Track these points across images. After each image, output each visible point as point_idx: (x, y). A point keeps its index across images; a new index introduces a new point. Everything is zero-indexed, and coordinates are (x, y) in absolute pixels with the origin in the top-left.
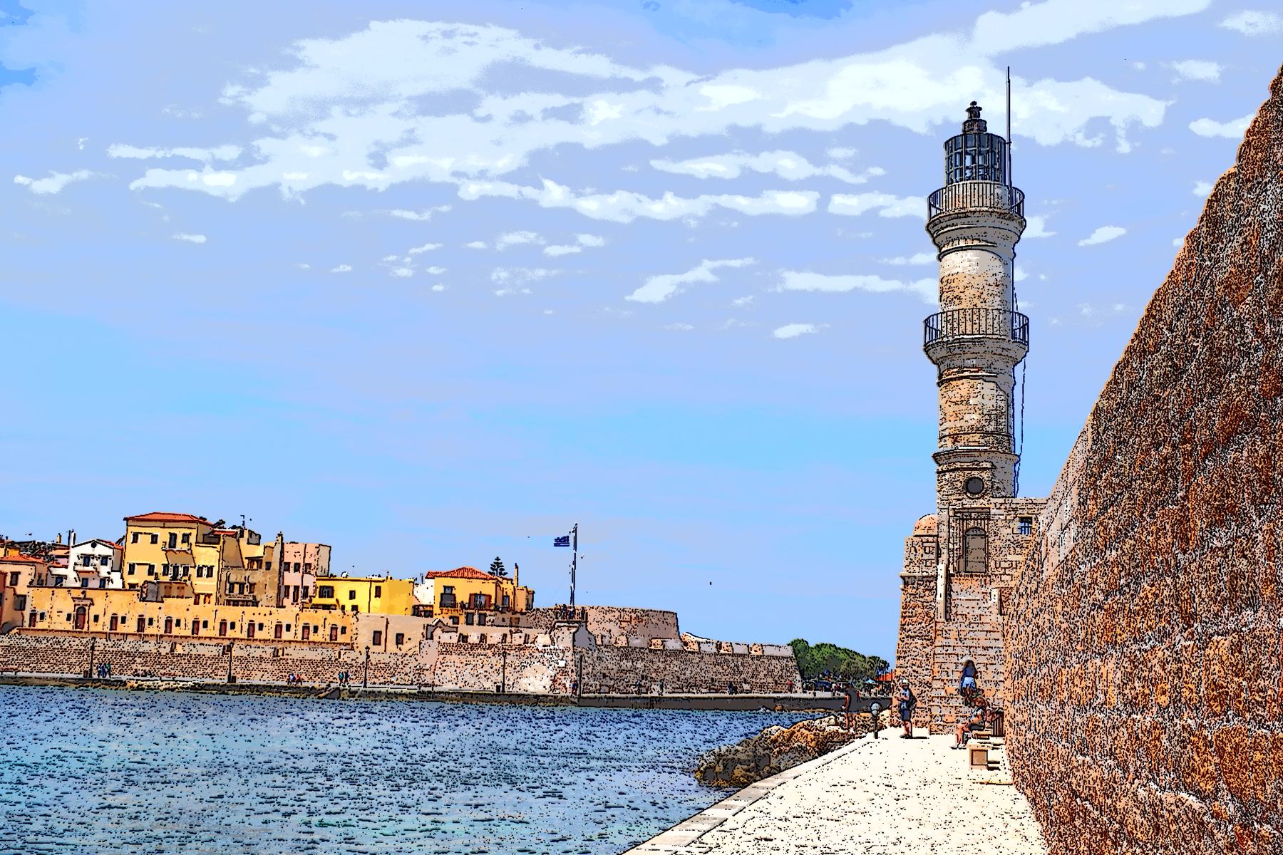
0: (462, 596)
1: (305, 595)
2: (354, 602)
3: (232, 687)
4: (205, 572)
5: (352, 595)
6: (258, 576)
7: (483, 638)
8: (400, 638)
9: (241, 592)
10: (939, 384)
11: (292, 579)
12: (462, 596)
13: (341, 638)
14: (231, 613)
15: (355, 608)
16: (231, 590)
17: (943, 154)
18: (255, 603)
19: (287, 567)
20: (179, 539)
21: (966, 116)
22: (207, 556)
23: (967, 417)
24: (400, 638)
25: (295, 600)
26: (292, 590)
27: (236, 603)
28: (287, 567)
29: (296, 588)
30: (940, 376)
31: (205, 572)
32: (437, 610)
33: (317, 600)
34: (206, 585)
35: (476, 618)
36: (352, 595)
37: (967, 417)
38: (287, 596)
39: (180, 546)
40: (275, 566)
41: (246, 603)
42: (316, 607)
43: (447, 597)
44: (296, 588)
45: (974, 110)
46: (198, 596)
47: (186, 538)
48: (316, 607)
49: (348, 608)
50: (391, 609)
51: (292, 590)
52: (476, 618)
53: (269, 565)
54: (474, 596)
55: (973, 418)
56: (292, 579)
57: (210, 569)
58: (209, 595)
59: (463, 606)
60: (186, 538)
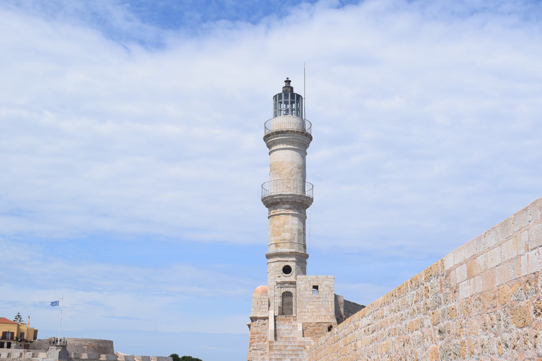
7: (9, 355)
10: (269, 218)
17: (272, 102)
21: (284, 84)
23: (283, 234)
30: (269, 214)
35: (5, 345)
37: (283, 234)
45: (288, 82)
52: (5, 345)
55: (287, 236)
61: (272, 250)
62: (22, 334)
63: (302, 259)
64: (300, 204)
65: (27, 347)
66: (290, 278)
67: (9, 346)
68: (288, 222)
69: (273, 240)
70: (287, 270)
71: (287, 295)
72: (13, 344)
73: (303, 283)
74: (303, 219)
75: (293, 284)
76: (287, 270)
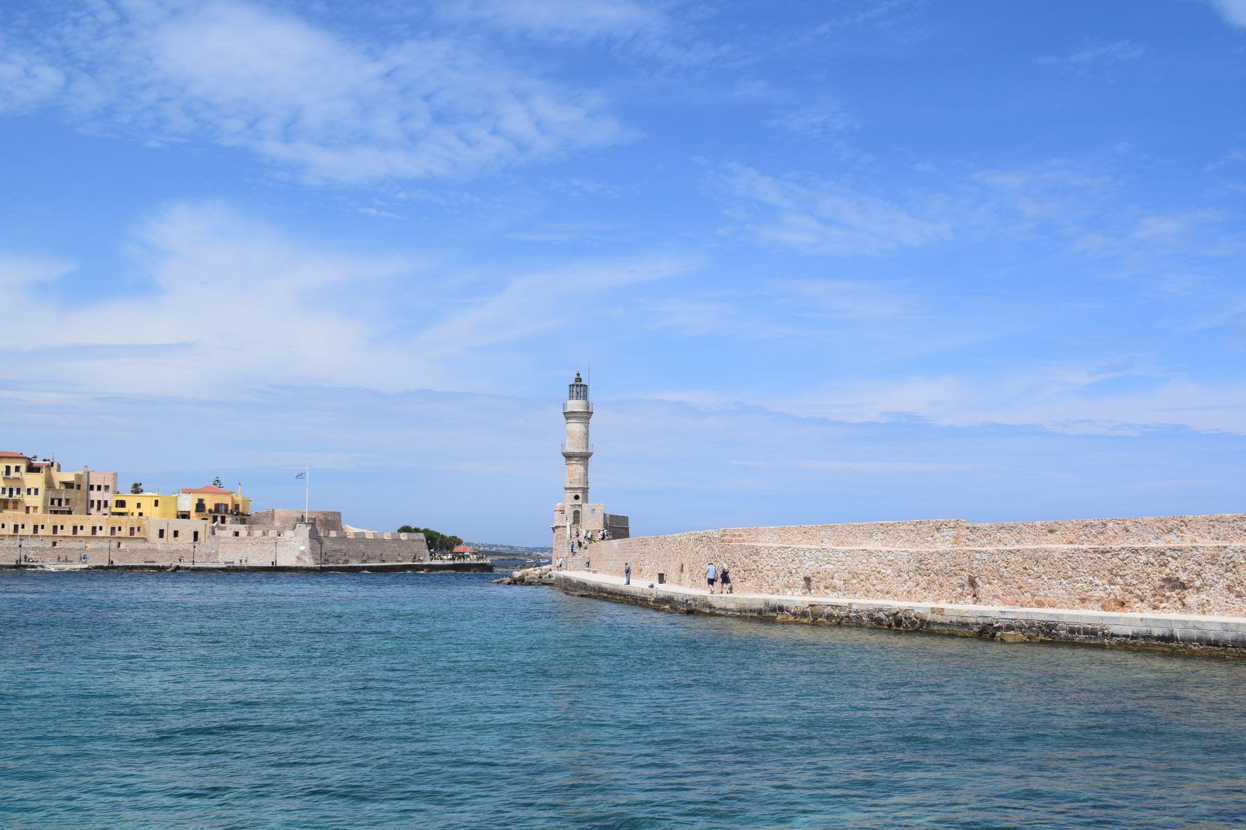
0: (209, 505)
1: (106, 505)
2: (140, 510)
3: (111, 567)
4: (33, 491)
5: (139, 505)
6: (72, 494)
8: (176, 534)
9: (60, 504)
11: (95, 495)
12: (209, 505)
13: (137, 534)
14: (59, 519)
15: (141, 514)
16: (52, 503)
18: (70, 512)
19: (92, 488)
20: (13, 470)
22: (35, 480)
24: (176, 534)
25: (99, 509)
26: (96, 504)
27: (56, 512)
28: (92, 488)
29: (99, 502)
31: (33, 491)
32: (193, 514)
33: (115, 510)
34: (30, 500)
36: (139, 505)
38: (92, 506)
39: (13, 474)
40: (84, 487)
41: (63, 512)
42: (114, 514)
43: (200, 507)
44: (99, 502)
46: (28, 508)
47: (17, 469)
48: (114, 514)
49: (136, 514)
50: (164, 515)
51: (96, 504)
53: (79, 487)
54: (217, 506)
55: (577, 477)
56: (95, 495)
57: (36, 490)
58: (35, 508)
59: (210, 511)
60: (17, 469)
61: (568, 485)
62: (237, 506)
63: (585, 490)
64: (585, 457)
65: (243, 522)
66: (579, 502)
67: (223, 521)
68: (578, 468)
69: (568, 479)
70: (577, 497)
71: (576, 513)
72: (228, 519)
73: (586, 509)
74: (586, 468)
75: (580, 506)
76: (577, 497)
